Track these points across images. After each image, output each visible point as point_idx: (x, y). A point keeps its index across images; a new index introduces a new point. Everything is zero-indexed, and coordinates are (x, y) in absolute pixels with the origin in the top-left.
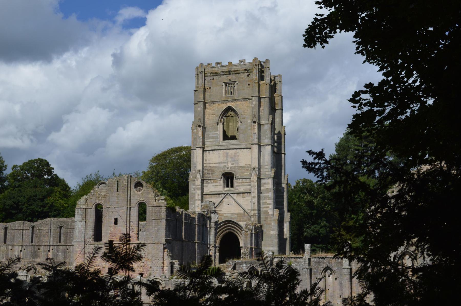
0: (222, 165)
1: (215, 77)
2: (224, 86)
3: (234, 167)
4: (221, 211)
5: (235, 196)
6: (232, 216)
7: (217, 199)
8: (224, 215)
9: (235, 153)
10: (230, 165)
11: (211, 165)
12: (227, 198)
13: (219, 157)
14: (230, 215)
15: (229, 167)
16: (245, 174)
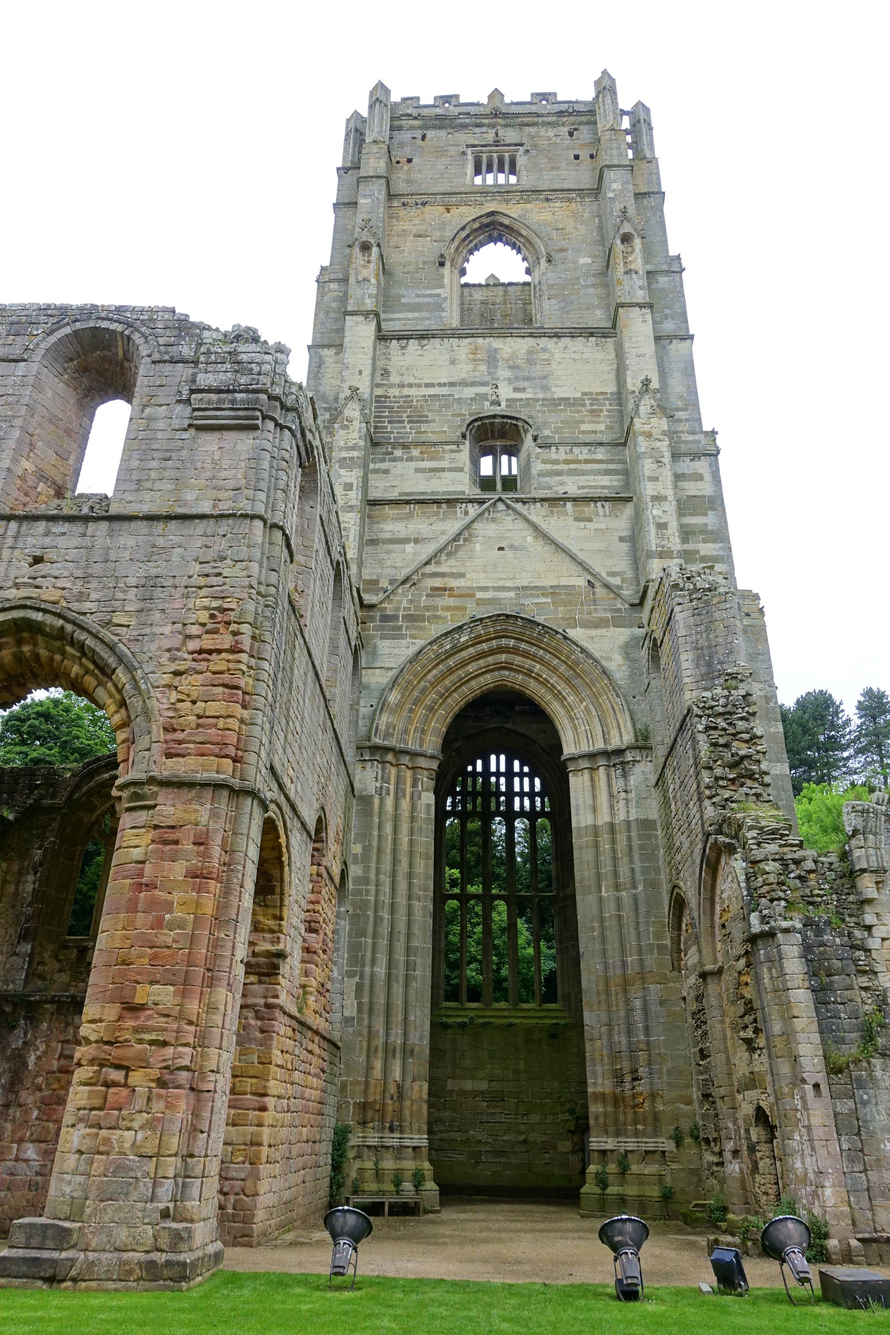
0: (469, 392)
1: (430, 134)
2: (470, 157)
3: (528, 403)
4: (462, 575)
5: (536, 513)
6: (523, 601)
7: (439, 526)
8: (480, 595)
9: (530, 352)
10: (505, 392)
11: (413, 392)
12: (494, 520)
13: (453, 362)
14: (512, 594)
15: (506, 396)
16: (584, 427)
